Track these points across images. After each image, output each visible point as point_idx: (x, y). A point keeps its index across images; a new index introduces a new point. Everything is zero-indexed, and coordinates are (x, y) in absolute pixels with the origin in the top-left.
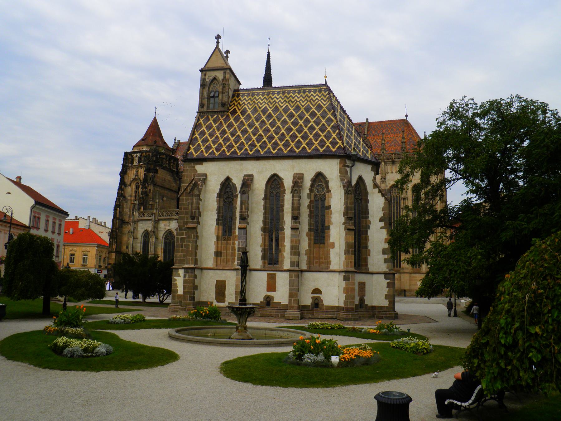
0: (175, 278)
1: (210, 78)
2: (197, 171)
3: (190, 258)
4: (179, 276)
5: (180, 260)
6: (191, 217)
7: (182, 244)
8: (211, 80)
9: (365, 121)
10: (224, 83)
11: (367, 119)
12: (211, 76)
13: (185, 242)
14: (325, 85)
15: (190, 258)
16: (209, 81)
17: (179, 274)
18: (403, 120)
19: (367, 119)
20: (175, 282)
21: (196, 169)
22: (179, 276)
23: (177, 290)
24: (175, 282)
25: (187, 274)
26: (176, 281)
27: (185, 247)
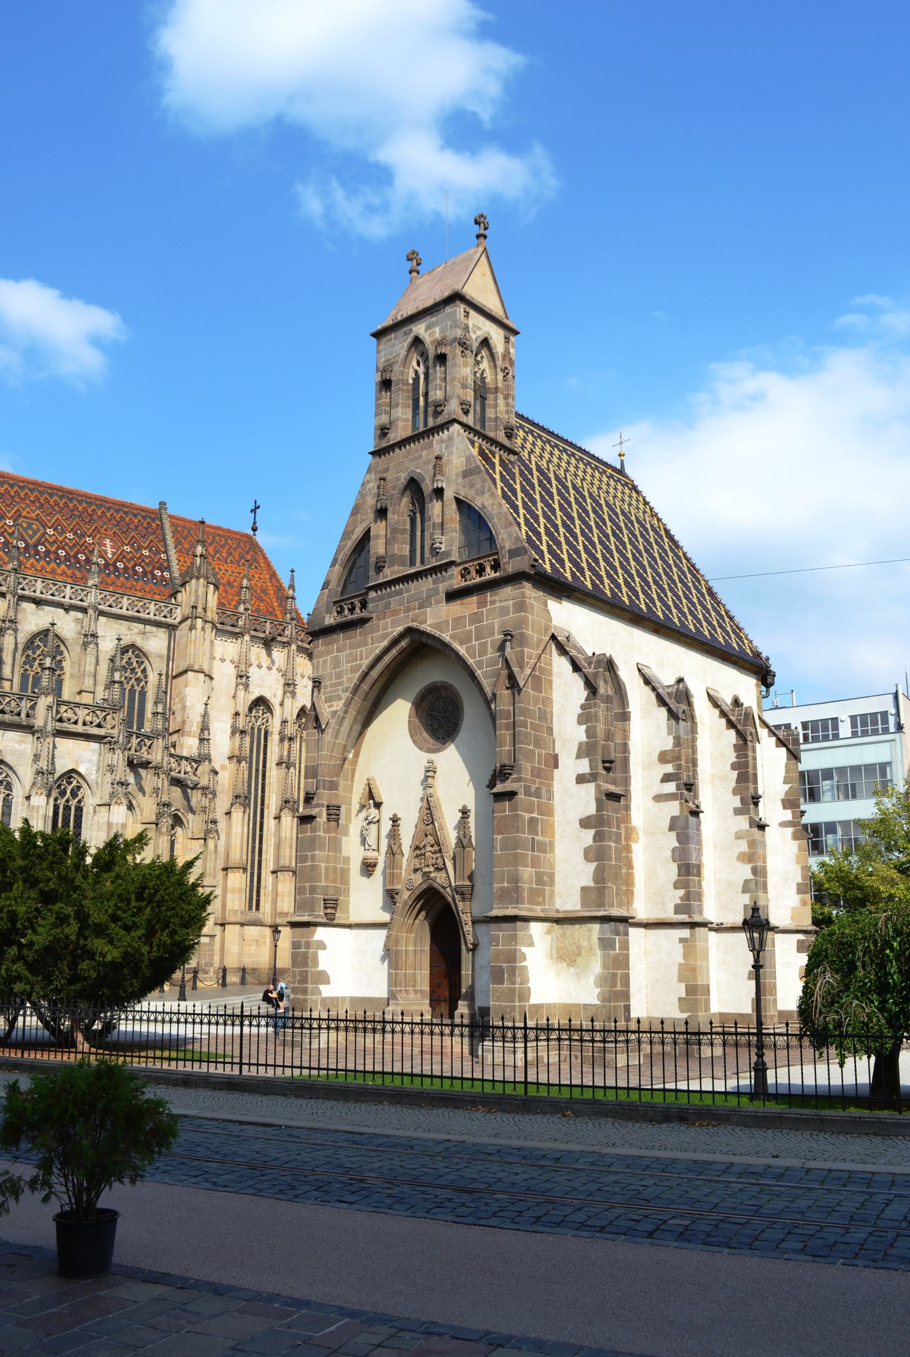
0: (524, 949)
1: (479, 333)
2: (550, 620)
3: (615, 887)
4: (532, 944)
5: (531, 889)
6: (604, 762)
7: (533, 839)
8: (479, 341)
9: (155, 506)
10: (506, 368)
11: (163, 504)
12: (479, 329)
13: (537, 834)
14: (621, 472)
15: (615, 887)
16: (476, 339)
17: (531, 936)
18: (247, 536)
19: (163, 504)
20: (523, 964)
21: (548, 611)
22: (532, 944)
23: (529, 989)
24: (523, 964)
25: (617, 938)
26: (525, 960)
27: (538, 851)
